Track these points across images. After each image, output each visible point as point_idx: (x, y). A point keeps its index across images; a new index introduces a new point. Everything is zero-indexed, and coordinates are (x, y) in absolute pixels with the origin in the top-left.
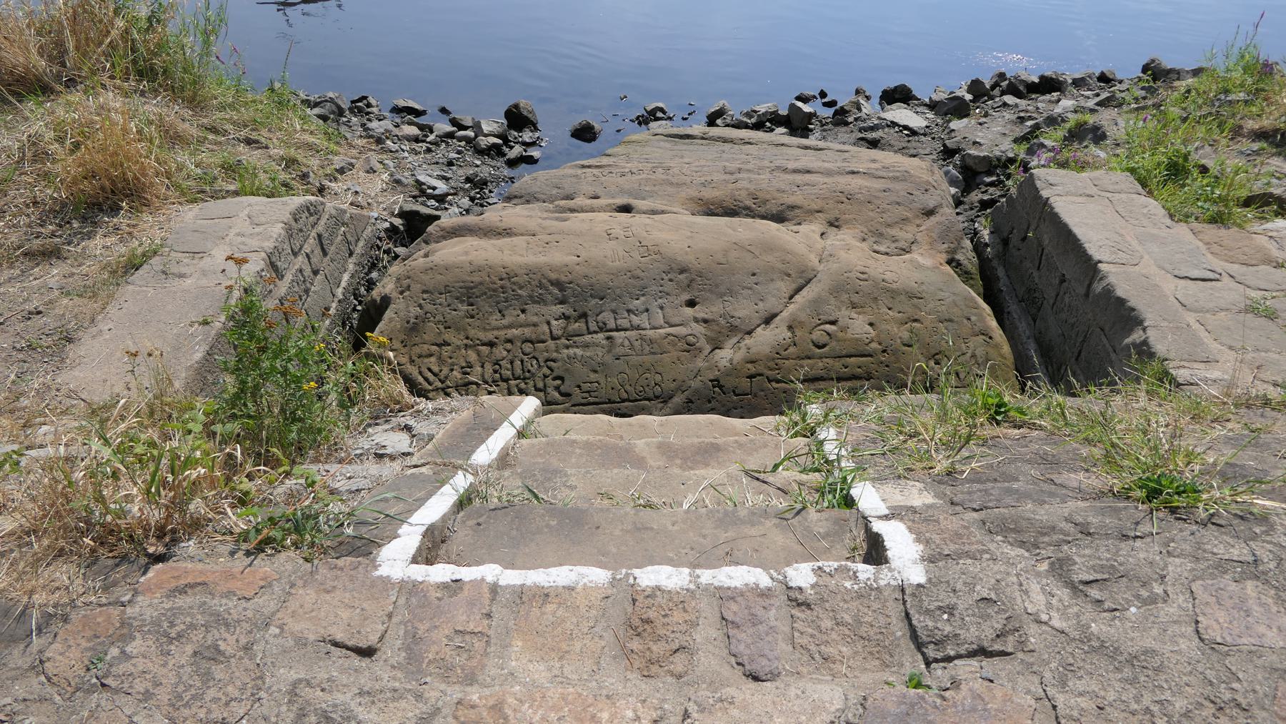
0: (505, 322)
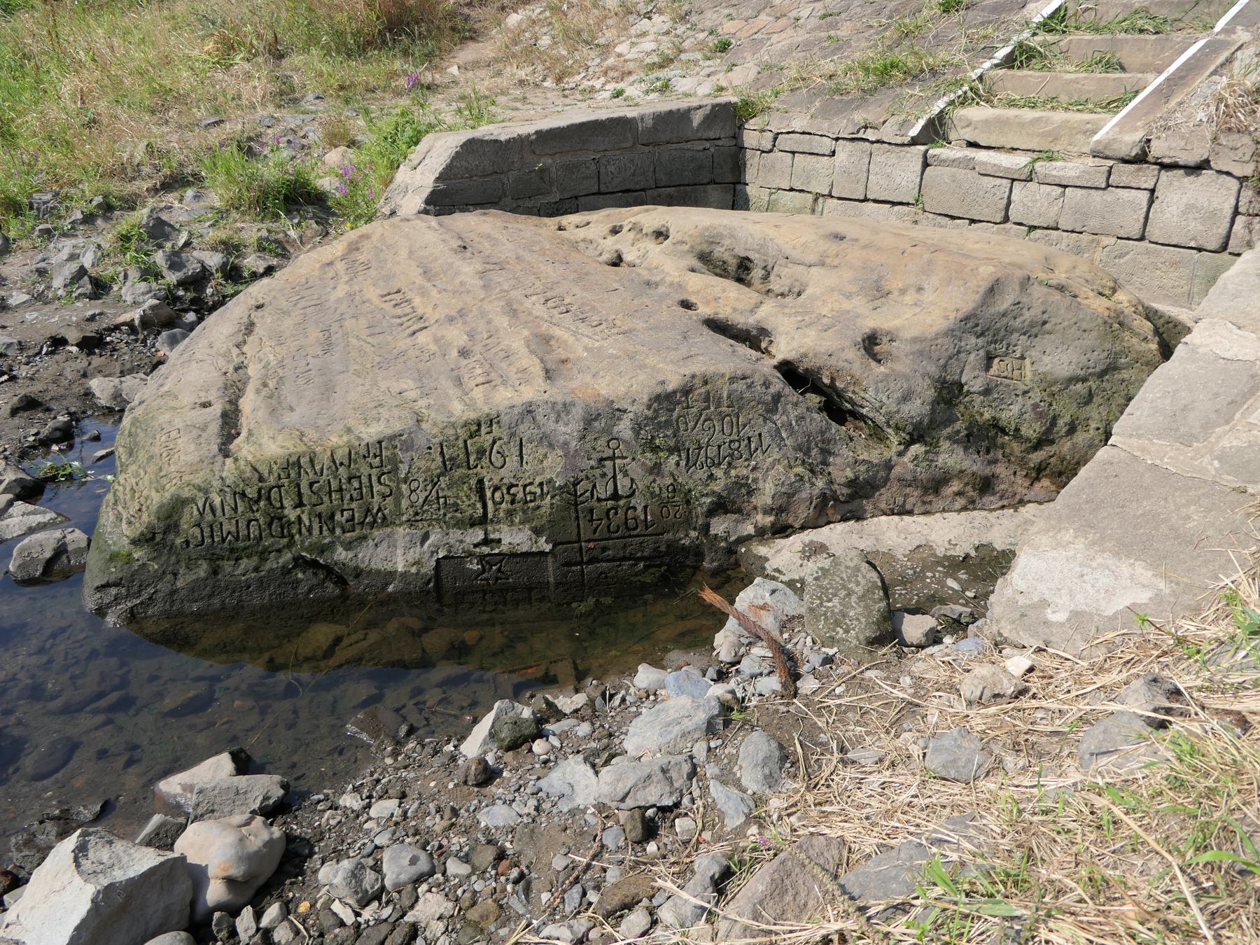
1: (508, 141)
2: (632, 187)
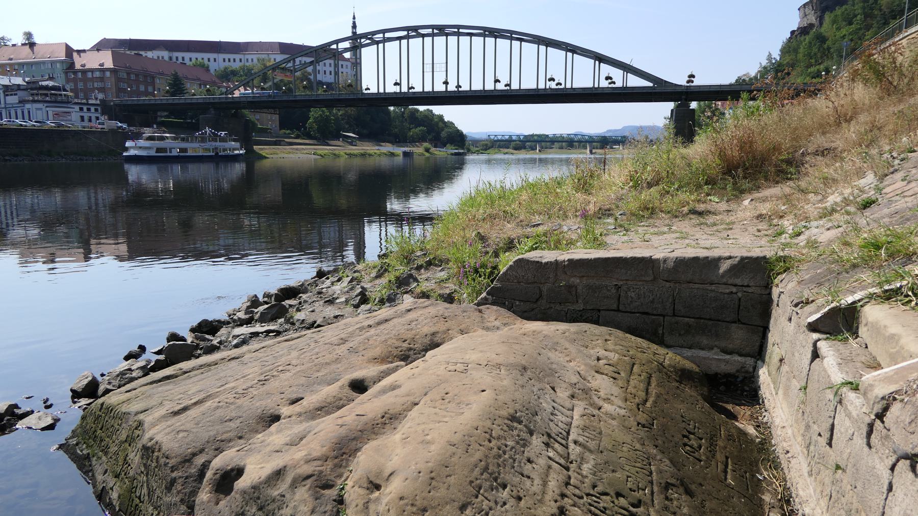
0: (537, 481)
1: (547, 263)
2: (649, 311)
